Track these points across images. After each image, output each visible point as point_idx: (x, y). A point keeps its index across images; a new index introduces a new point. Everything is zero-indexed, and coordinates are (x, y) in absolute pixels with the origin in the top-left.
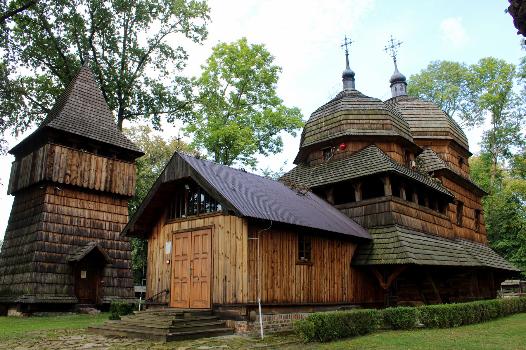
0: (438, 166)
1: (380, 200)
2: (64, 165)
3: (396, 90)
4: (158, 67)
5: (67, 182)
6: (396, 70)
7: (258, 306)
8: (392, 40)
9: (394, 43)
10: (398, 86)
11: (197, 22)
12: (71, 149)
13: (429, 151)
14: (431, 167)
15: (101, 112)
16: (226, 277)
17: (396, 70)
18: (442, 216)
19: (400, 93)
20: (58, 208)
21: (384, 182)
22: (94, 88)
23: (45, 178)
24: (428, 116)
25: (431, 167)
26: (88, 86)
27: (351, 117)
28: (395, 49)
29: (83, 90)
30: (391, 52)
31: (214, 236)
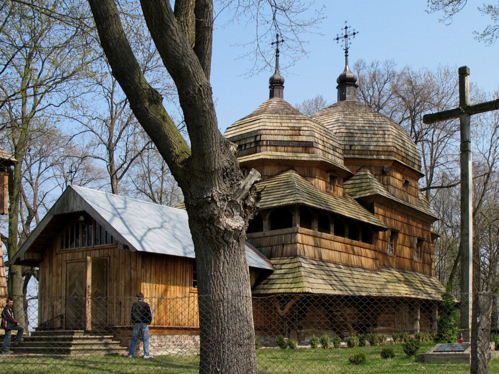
8: (346, 28)
9: (348, 31)
16: (121, 303)
28: (348, 41)
30: (344, 43)
31: (109, 266)
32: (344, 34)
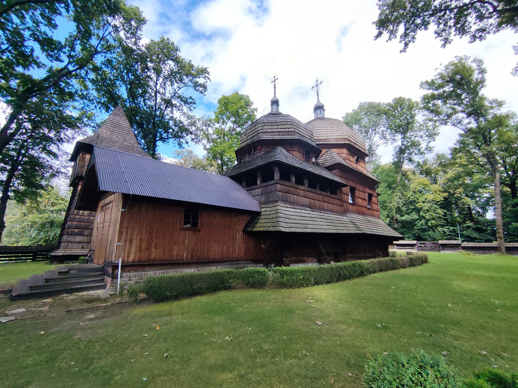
0: (335, 161)
1: (271, 183)
3: (317, 114)
4: (179, 110)
7: (118, 266)
8: (317, 81)
10: (318, 111)
13: (331, 152)
14: (330, 163)
18: (333, 196)
19: (319, 116)
22: (123, 120)
23: (77, 175)
24: (333, 128)
25: (330, 163)
26: (119, 118)
27: (266, 127)
29: (114, 121)
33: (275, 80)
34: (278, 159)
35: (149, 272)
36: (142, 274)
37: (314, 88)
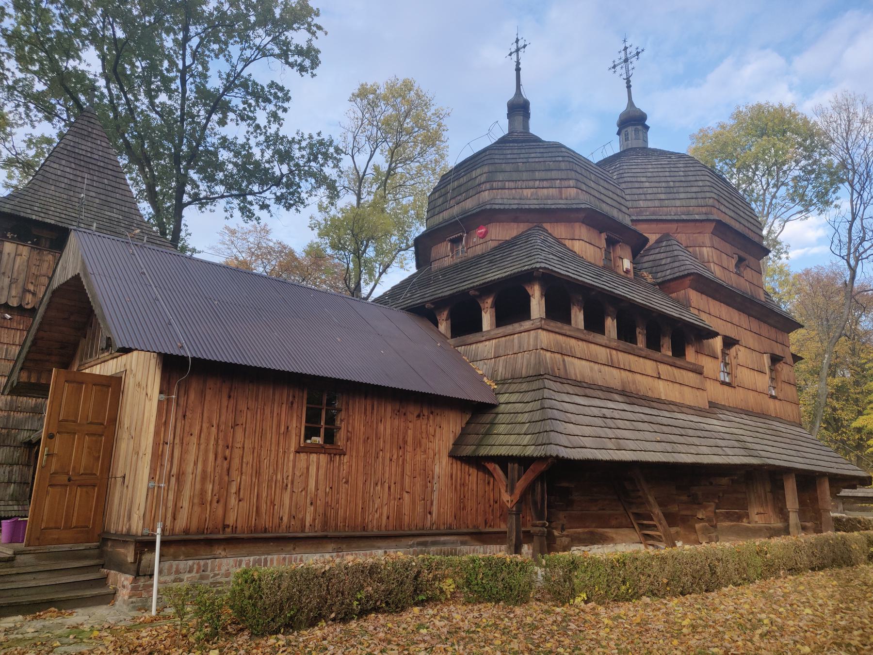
0: (683, 268)
1: (522, 329)
2: (22, 277)
3: (627, 139)
5: (28, 304)
6: (631, 103)
8: (626, 48)
9: (628, 53)
10: (630, 130)
11: (298, 37)
12: (37, 249)
13: (669, 243)
14: (668, 272)
15: (109, 188)
17: (631, 103)
19: (632, 144)
20: (7, 349)
21: (531, 294)
22: (101, 148)
24: (673, 179)
25: (668, 272)
26: (89, 144)
29: (77, 151)
32: (624, 58)
33: (518, 50)
34: (543, 265)
35: (225, 561)
36: (206, 565)
37: (618, 68)
